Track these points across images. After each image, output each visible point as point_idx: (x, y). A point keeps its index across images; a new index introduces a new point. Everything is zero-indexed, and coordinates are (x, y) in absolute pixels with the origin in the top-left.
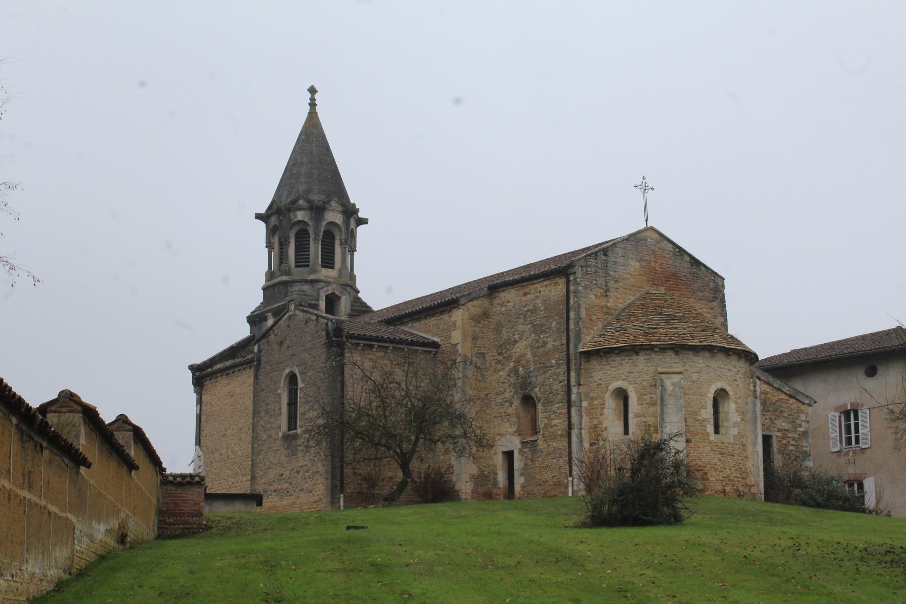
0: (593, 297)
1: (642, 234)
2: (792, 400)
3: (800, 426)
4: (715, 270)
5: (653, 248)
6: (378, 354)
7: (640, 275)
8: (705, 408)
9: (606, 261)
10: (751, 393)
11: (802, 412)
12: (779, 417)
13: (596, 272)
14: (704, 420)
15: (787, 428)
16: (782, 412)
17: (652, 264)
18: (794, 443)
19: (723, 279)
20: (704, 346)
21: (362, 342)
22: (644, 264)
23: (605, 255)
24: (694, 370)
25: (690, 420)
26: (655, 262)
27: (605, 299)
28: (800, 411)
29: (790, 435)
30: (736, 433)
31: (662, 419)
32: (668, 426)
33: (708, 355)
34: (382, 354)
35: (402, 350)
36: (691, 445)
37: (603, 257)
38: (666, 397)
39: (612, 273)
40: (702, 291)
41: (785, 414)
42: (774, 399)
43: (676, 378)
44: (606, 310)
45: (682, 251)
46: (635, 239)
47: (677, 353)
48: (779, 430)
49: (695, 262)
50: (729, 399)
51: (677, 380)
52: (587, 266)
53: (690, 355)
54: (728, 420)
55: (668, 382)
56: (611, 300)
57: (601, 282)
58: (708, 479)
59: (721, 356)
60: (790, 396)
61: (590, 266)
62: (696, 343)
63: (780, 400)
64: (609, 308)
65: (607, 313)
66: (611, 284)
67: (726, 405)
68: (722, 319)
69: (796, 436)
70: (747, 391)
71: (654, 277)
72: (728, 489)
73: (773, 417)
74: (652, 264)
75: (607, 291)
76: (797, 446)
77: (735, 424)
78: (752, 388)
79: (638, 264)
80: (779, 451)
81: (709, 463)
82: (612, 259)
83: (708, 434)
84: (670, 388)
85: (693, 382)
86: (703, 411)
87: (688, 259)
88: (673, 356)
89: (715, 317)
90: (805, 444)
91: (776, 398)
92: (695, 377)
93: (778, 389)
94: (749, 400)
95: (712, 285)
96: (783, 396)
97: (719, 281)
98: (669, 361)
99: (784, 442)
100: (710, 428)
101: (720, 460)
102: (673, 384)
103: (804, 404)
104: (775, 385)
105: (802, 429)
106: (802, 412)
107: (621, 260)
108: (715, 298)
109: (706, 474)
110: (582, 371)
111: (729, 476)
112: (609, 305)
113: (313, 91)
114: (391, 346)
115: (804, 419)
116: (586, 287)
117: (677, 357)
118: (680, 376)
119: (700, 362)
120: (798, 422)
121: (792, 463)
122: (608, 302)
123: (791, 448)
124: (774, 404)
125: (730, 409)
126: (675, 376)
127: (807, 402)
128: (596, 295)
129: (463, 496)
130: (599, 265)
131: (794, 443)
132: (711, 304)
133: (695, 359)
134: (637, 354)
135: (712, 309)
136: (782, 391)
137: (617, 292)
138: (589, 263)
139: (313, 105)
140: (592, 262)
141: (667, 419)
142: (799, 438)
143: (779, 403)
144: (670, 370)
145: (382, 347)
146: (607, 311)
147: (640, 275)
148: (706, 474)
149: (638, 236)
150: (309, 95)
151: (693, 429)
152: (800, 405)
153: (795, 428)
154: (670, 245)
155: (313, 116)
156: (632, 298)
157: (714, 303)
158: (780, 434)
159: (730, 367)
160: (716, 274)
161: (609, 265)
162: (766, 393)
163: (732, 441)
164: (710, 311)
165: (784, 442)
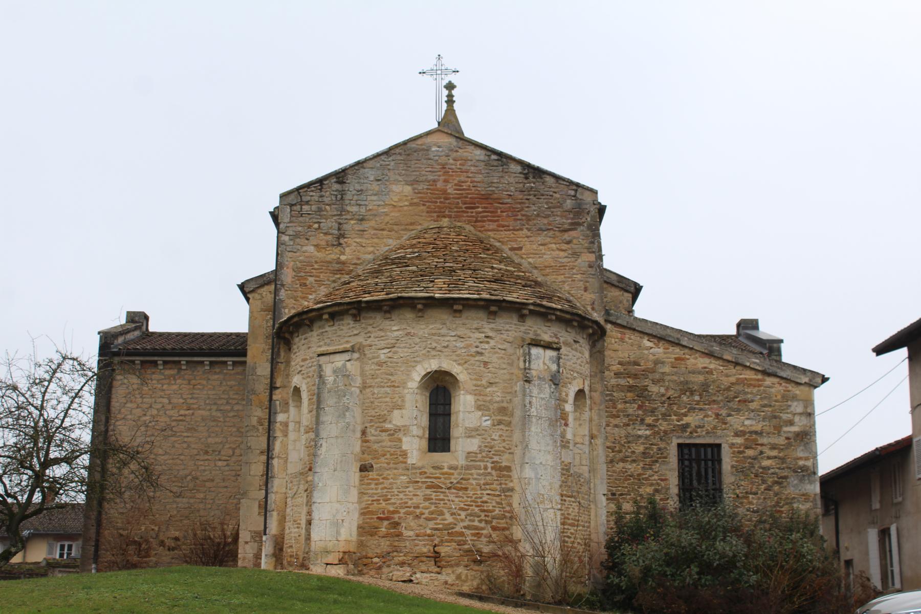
0: (311, 249)
1: (419, 142)
2: (769, 381)
3: (791, 423)
4: (575, 179)
5: (443, 160)
6: (167, 372)
7: (411, 204)
8: (400, 408)
9: (343, 193)
10: (520, 374)
11: (794, 398)
12: (738, 410)
13: (320, 210)
14: (398, 430)
15: (758, 428)
16: (745, 401)
17: (440, 185)
18: (774, 453)
19: (594, 192)
20: (391, 299)
21: (138, 359)
22: (420, 187)
23: (341, 182)
24: (383, 344)
25: (371, 431)
26: (446, 181)
27: (337, 250)
28: (787, 398)
29: (765, 440)
30: (475, 448)
31: (317, 435)
32: (324, 444)
33: (409, 315)
34: (173, 372)
35: (133, 362)
36: (372, 475)
37: (336, 186)
38: (325, 395)
39: (354, 209)
40: (547, 217)
41: (753, 406)
42: (726, 381)
43: (339, 361)
44: (337, 266)
45: (503, 158)
46: (404, 152)
47: (356, 318)
48: (737, 434)
49: (533, 172)
50: (459, 387)
51: (339, 364)
52: (301, 203)
53: (378, 318)
54: (458, 426)
55: (328, 370)
56: (347, 250)
57: (330, 224)
58: (399, 535)
59: (444, 315)
60: (765, 373)
61: (307, 203)
62: (382, 296)
63: (739, 382)
64: (344, 263)
65: (340, 271)
66: (351, 226)
67: (457, 398)
68: (592, 257)
69: (781, 441)
70: (516, 371)
71: (438, 203)
72: (444, 550)
73: (724, 412)
74: (440, 185)
75: (342, 236)
76: (783, 460)
77: (471, 433)
78: (522, 365)
79: (408, 189)
80: (739, 470)
81: (404, 505)
82: (353, 185)
83: (405, 454)
84: (330, 379)
85: (380, 364)
86: (396, 412)
87: (519, 168)
88: (352, 322)
89: (576, 255)
90: (801, 454)
91: (733, 379)
92: (383, 355)
93: (736, 364)
94: (518, 387)
95: (569, 203)
96: (748, 375)
97: (587, 197)
98: (347, 332)
99: (750, 453)
100: (414, 445)
101: (427, 499)
102: (335, 372)
103: (800, 384)
104: (725, 357)
105: (795, 429)
106: (794, 398)
107: (375, 187)
108: (575, 226)
109: (396, 525)
110: (282, 366)
111: (448, 527)
112: (343, 258)
113: (450, 87)
114: (184, 360)
115: (800, 409)
116: (296, 236)
117: (357, 325)
118: (346, 356)
119: (395, 328)
120: (785, 416)
121: (768, 489)
122: (343, 254)
123: (766, 463)
124: (728, 389)
125: (464, 407)
126: (337, 357)
127: (805, 379)
128: (316, 246)
129: (240, 563)
130: (327, 200)
131: (774, 453)
132: (566, 236)
133: (388, 322)
134: (310, 326)
135: (569, 242)
136: (746, 366)
137: (361, 236)
138: (305, 199)
139: (450, 101)
140: (314, 195)
141: (323, 434)
142: (789, 445)
143: (737, 387)
144: (331, 349)
145: (174, 362)
146: (341, 268)
147: (411, 204)
148: (396, 525)
149: (412, 145)
150: (445, 92)
151: (376, 446)
152: (790, 387)
153: (778, 429)
154: (478, 152)
155: (450, 111)
156: (393, 243)
157: (573, 234)
158: (739, 440)
159: (462, 331)
160: (578, 185)
161: (348, 196)
162: (710, 372)
163: (462, 462)
164: (565, 247)
165: (750, 453)
